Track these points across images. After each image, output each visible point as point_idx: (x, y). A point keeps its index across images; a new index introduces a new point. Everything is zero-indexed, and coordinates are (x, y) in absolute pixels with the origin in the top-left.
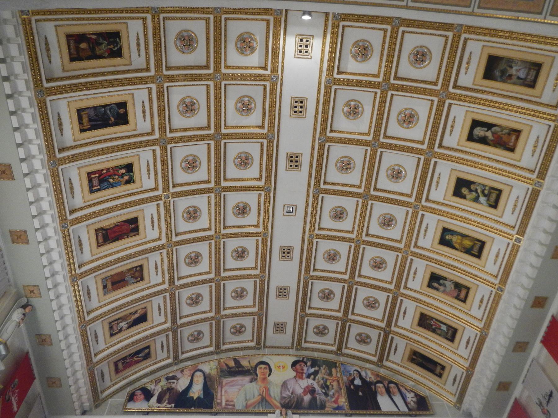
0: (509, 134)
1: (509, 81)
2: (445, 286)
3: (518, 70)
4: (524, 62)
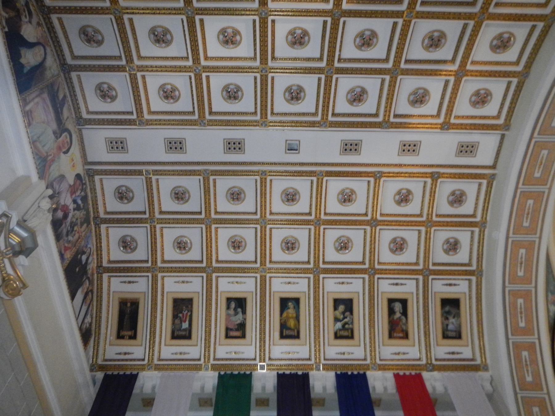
0: (402, 331)
1: (443, 319)
2: (236, 313)
3: (453, 323)
4: (460, 326)
